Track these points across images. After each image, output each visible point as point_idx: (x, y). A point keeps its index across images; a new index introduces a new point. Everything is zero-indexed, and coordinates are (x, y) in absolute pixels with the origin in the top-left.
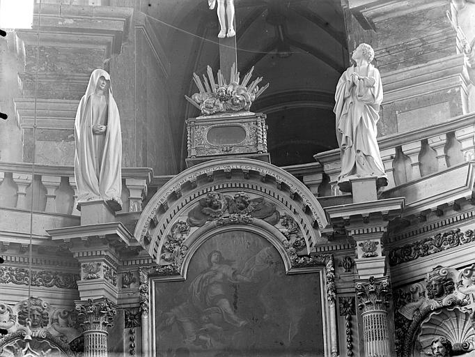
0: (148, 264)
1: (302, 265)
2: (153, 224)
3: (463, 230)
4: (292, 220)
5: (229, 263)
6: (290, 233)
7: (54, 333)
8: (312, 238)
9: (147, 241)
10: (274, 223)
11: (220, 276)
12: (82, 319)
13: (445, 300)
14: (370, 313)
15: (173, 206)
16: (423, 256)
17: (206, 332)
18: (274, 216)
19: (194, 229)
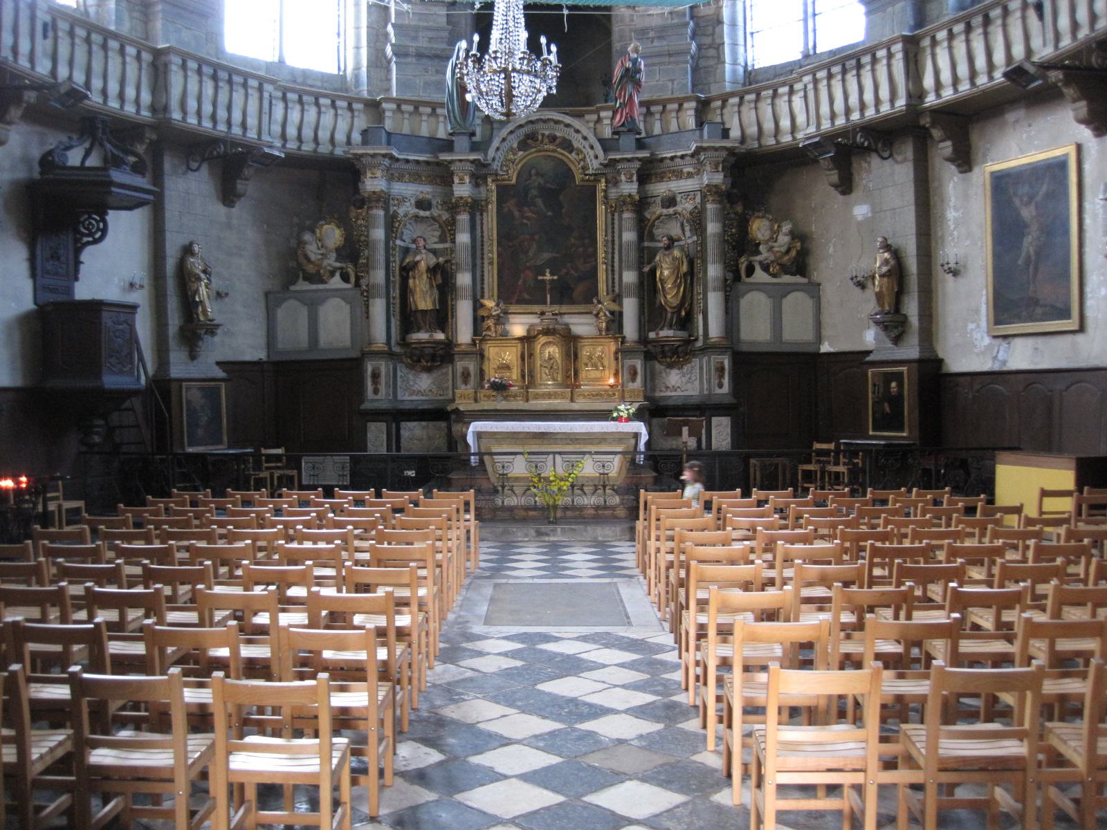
1: (588, 180)
2: (498, 149)
3: (685, 170)
5: (542, 176)
7: (436, 214)
8: (594, 165)
10: (571, 152)
13: (671, 210)
14: (626, 215)
15: (512, 136)
19: (521, 153)
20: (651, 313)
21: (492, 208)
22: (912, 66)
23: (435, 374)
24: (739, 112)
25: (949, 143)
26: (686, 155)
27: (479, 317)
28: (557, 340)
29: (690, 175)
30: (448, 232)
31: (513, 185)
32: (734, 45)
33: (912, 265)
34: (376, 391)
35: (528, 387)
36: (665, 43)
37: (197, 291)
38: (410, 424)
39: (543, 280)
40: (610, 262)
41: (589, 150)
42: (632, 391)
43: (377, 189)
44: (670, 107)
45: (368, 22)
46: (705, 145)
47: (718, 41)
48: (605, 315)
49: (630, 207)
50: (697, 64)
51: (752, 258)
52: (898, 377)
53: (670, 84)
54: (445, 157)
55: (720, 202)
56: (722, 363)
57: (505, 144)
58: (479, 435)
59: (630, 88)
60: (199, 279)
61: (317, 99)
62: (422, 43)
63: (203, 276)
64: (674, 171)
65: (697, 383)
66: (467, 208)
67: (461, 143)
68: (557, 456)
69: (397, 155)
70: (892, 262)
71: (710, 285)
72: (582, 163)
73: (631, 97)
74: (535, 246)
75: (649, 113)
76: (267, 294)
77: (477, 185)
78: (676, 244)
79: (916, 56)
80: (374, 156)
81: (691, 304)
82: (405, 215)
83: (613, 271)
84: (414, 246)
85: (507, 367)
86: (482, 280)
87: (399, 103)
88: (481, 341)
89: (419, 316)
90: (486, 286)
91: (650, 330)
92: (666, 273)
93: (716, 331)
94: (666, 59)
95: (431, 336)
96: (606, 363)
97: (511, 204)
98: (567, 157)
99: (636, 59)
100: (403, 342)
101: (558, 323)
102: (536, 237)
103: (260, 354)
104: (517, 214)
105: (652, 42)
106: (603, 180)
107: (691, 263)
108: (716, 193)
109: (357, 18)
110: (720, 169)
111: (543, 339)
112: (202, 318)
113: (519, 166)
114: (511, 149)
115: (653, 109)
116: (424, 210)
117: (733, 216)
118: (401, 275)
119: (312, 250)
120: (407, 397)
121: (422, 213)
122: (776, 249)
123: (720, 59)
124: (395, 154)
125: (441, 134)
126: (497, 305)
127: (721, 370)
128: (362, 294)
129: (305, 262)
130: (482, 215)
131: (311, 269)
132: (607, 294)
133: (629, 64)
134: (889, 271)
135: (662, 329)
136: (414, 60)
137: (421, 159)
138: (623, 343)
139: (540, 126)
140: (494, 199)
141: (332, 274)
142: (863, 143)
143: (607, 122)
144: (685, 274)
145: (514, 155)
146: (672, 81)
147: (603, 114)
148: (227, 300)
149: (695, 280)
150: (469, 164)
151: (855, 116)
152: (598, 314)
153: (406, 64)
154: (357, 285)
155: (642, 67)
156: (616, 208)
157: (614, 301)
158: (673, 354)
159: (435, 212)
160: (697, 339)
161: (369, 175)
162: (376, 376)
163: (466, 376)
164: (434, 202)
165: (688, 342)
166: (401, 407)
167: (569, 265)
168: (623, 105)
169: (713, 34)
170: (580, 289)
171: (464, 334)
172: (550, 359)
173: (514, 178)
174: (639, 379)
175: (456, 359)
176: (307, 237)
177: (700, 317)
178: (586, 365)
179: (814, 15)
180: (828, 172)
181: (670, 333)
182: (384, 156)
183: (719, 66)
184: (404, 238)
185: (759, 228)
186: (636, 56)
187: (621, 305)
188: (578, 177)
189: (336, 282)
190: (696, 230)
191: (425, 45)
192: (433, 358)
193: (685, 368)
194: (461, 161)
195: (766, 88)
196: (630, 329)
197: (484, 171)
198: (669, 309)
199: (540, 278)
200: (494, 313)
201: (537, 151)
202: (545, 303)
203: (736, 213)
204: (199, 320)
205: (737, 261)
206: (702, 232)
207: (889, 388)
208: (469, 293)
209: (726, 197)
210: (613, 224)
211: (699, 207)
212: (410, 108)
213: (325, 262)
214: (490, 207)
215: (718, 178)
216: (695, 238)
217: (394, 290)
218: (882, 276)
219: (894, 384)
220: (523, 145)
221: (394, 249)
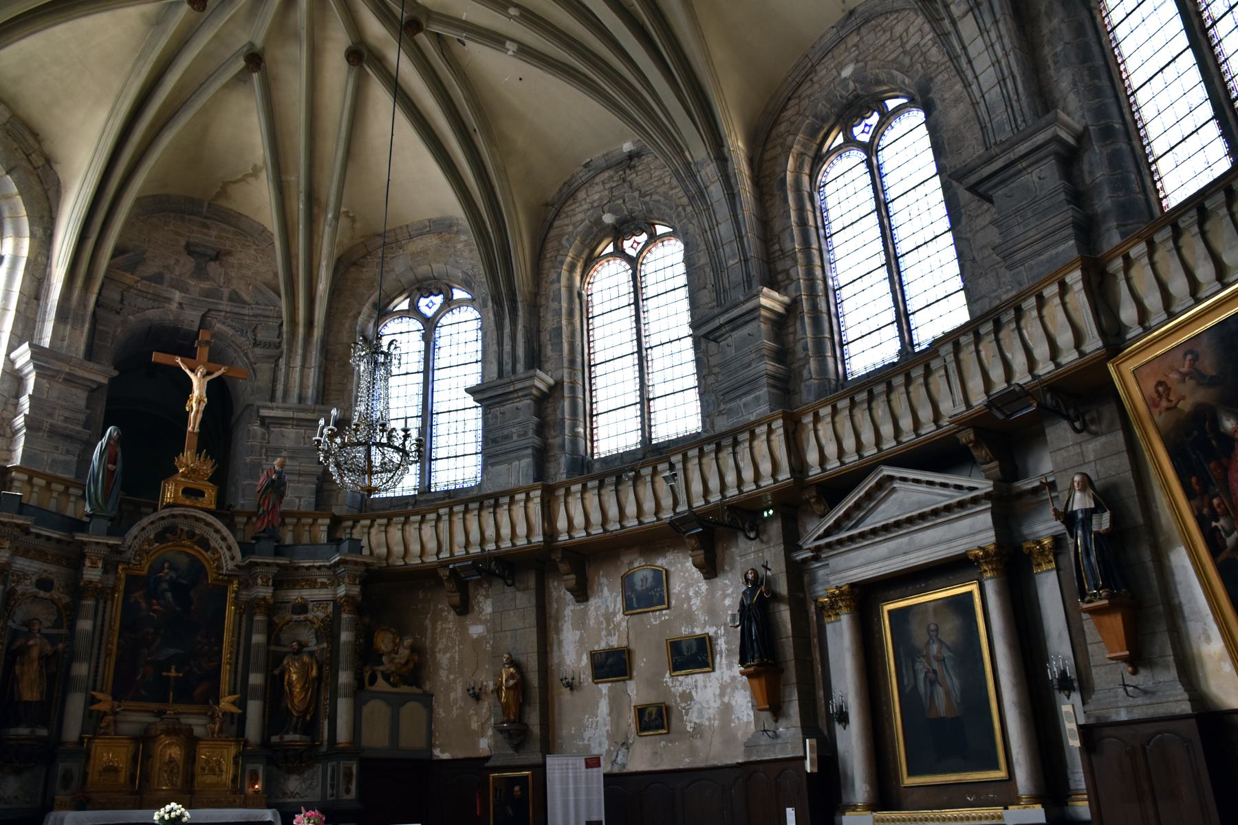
3: (319, 580)
4: (218, 552)
7: (56, 597)
8: (228, 565)
10: (207, 551)
11: (168, 577)
13: (302, 617)
14: (258, 618)
15: (151, 527)
19: (157, 545)
20: (276, 717)
22: (546, 510)
24: (369, 533)
25: (573, 576)
29: (324, 585)
30: (69, 615)
33: (534, 679)
36: (296, 463)
39: (168, 677)
51: (376, 668)
53: (297, 501)
54: (80, 537)
56: (350, 769)
62: (58, 420)
64: (308, 580)
65: (318, 789)
70: (518, 676)
71: (341, 691)
72: (216, 563)
78: (305, 649)
79: (549, 502)
82: (23, 594)
83: (236, 672)
84: (26, 629)
85: (115, 770)
92: (294, 677)
93: (343, 734)
97: (138, 595)
98: (203, 555)
104: (144, 605)
106: (236, 582)
107: (320, 669)
110: (357, 582)
115: (287, 520)
121: (42, 593)
127: (348, 775)
130: (105, 602)
134: (516, 684)
135: (287, 733)
138: (244, 746)
140: (122, 587)
145: (149, 545)
146: (300, 498)
149: (323, 685)
151: (491, 547)
156: (248, 609)
159: (55, 594)
163: (67, 778)
171: (73, 730)
173: (146, 568)
177: (326, 722)
180: (450, 594)
181: (297, 737)
185: (384, 642)
194: (98, 543)
195: (399, 515)
199: (165, 674)
201: (174, 545)
211: (331, 616)
212: (42, 482)
215: (356, 590)
219: (517, 788)
220: (160, 537)
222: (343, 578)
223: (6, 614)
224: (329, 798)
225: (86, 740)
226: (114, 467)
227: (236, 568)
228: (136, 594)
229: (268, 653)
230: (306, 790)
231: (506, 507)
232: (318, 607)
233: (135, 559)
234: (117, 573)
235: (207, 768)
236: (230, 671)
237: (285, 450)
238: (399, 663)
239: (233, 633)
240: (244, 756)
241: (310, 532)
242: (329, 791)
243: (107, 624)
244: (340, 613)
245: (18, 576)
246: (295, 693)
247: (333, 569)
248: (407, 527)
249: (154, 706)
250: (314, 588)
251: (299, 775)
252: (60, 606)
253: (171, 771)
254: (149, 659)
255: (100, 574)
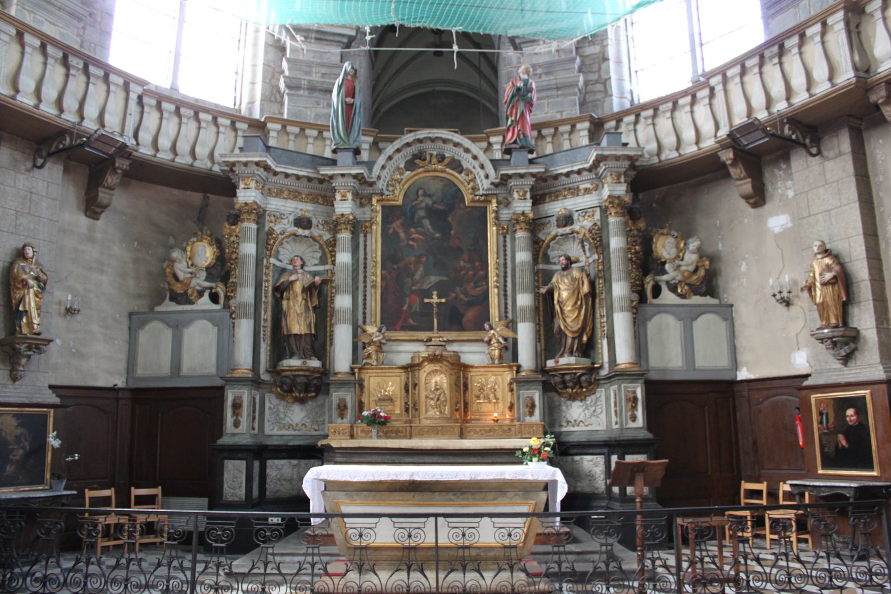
0: (378, 194)
1: (478, 201)
2: (383, 167)
3: (582, 187)
4: (472, 173)
5: (430, 196)
6: (471, 181)
7: (316, 234)
8: (484, 185)
9: (379, 177)
10: (460, 173)
11: (423, 205)
12: (336, 226)
13: (567, 229)
14: (520, 234)
16: (554, 201)
17: (413, 239)
18: (460, 169)
19: (408, 173)
21: (377, 228)
22: (854, 37)
23: (310, 404)
24: (635, 131)
26: (584, 169)
27: (360, 345)
28: (445, 368)
29: (587, 191)
30: (329, 250)
31: (399, 206)
32: (620, 80)
33: (861, 270)
34: (236, 424)
35: (411, 422)
36: (552, 77)
37: (22, 300)
38: (276, 462)
39: (430, 304)
40: (502, 287)
41: (479, 169)
42: (531, 425)
43: (250, 200)
44: (562, 129)
45: (265, 60)
46: (606, 153)
47: (604, 76)
48: (499, 342)
49: (523, 225)
50: (584, 99)
51: (658, 278)
52: (859, 404)
54: (326, 171)
55: (623, 215)
56: (634, 392)
57: (391, 163)
58: (329, 486)
59: (521, 106)
60: (26, 285)
61: (196, 114)
62: (316, 77)
63: (31, 282)
64: (570, 189)
65: (603, 416)
66: (349, 227)
67: (345, 158)
68: (440, 519)
69: (273, 167)
70: (837, 268)
71: (616, 305)
72: (472, 184)
73: (522, 114)
74: (421, 268)
75: (540, 137)
76: (130, 315)
77: (362, 205)
78: (573, 265)
79: (858, 26)
80: (246, 164)
81: (593, 329)
82: (283, 233)
83: (505, 295)
84: (291, 267)
85: (390, 399)
86: (365, 304)
87: (285, 124)
88: (360, 369)
89: (292, 341)
90: (368, 311)
91: (547, 359)
92: (565, 294)
93: (624, 356)
94: (555, 93)
95: (304, 363)
96: (499, 394)
99: (528, 80)
100: (274, 369)
101: (446, 350)
102: (423, 260)
103: (120, 383)
104: (402, 235)
105: (540, 77)
106: (494, 201)
107: (592, 284)
108: (619, 205)
109: (255, 56)
110: (622, 180)
111: (428, 367)
112: (25, 330)
113: (406, 186)
114: (398, 169)
115: (544, 132)
116: (304, 228)
117: (635, 232)
118: (274, 295)
119: (182, 269)
120: (276, 432)
121: (300, 231)
122: (683, 268)
123: (607, 93)
124: (270, 162)
125: (328, 154)
126: (380, 331)
128: (231, 316)
129: (173, 281)
130: (365, 236)
131: (178, 288)
132: (500, 320)
133: (520, 84)
134: (835, 277)
135: (562, 356)
136: (306, 93)
137: (301, 173)
138: (518, 372)
139: (427, 145)
140: (379, 219)
141: (201, 294)
142: (791, 136)
143: (497, 147)
144: (586, 295)
145: (401, 174)
147: (493, 139)
148: (79, 317)
149: (597, 301)
150: (351, 180)
152: (490, 340)
153: (298, 96)
154: (227, 306)
155: (534, 86)
157: (507, 326)
158: (575, 384)
159: (315, 232)
160: (601, 367)
161: (242, 185)
162: (237, 406)
164: (314, 221)
165: (593, 370)
166: (269, 443)
167: (458, 288)
168: (515, 122)
169: (599, 70)
170: (470, 315)
171: (342, 359)
172: (437, 389)
173: (401, 198)
174: (537, 412)
175: (332, 390)
176: (176, 254)
178: (478, 397)
179: (702, 45)
180: (738, 182)
181: (572, 360)
182: (257, 164)
183: (607, 99)
184: (281, 257)
185: (664, 247)
186: (526, 77)
187: (515, 330)
188: (468, 198)
189: (205, 303)
190: (597, 248)
191: (317, 79)
192: (307, 388)
193: (589, 400)
194: (343, 175)
196: (526, 357)
197: (369, 190)
198: (569, 334)
199: (426, 300)
200: (375, 339)
202: (431, 329)
203: (639, 230)
204: (21, 333)
205: (642, 281)
206: (603, 250)
207: (845, 416)
208: (349, 316)
209: (631, 213)
210: (505, 246)
211: (599, 223)
212: (296, 130)
213: (194, 282)
214: (374, 227)
215: (621, 189)
216: (596, 257)
217: (266, 311)
218: (824, 284)
220: (411, 165)
221: (268, 268)
222: (605, 177)
223: (268, 253)
224: (615, 427)
225: (356, 370)
226: (352, 100)
227: (492, 187)
228: (394, 225)
229: (536, 273)
230: (590, 418)
231: (795, 50)
232: (584, 216)
233: (388, 190)
234: (372, 205)
235: (482, 396)
236: (498, 294)
237: (540, 67)
238: (685, 271)
239: (498, 254)
240: (519, 382)
241: (570, 140)
242: (614, 419)
243: (369, 256)
244: (607, 217)
245: (274, 216)
246: (566, 312)
247: (594, 171)
248: (677, 114)
249: (423, 335)
250: (578, 195)
251: (581, 400)
252: (321, 242)
253: (438, 399)
254: (414, 288)
255: (351, 206)
